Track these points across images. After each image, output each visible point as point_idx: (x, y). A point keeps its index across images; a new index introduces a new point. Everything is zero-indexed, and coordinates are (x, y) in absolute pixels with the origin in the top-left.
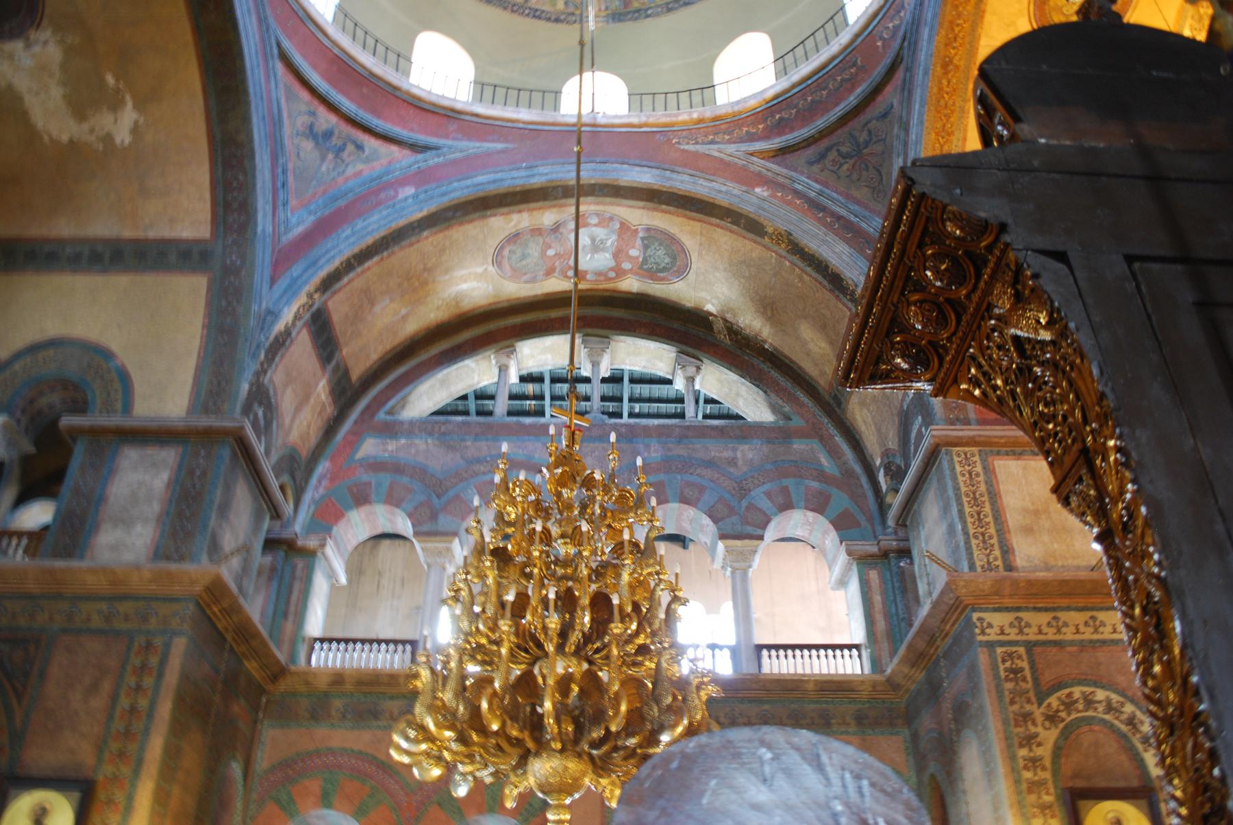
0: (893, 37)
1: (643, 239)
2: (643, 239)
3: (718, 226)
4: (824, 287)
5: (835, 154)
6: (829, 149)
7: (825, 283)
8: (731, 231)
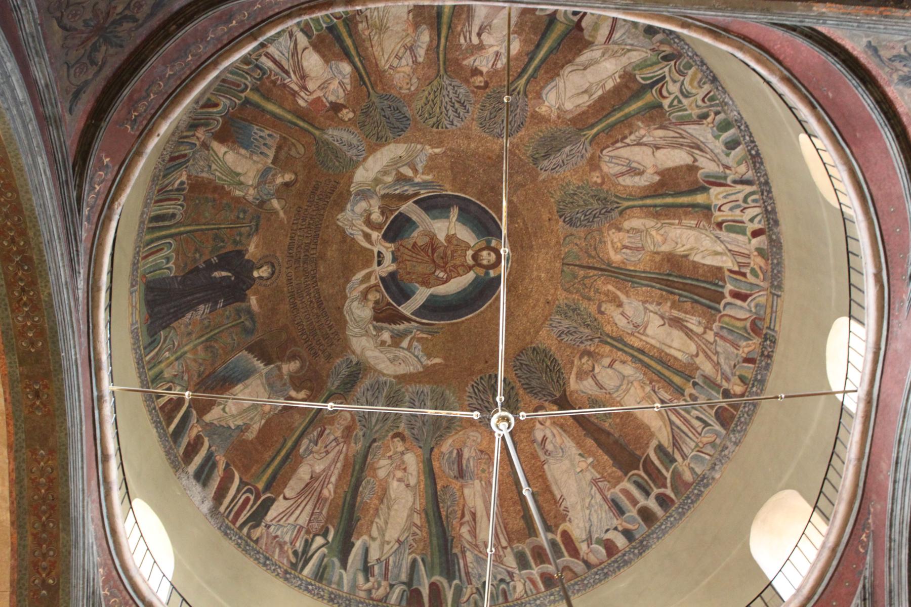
5: (138, 16)
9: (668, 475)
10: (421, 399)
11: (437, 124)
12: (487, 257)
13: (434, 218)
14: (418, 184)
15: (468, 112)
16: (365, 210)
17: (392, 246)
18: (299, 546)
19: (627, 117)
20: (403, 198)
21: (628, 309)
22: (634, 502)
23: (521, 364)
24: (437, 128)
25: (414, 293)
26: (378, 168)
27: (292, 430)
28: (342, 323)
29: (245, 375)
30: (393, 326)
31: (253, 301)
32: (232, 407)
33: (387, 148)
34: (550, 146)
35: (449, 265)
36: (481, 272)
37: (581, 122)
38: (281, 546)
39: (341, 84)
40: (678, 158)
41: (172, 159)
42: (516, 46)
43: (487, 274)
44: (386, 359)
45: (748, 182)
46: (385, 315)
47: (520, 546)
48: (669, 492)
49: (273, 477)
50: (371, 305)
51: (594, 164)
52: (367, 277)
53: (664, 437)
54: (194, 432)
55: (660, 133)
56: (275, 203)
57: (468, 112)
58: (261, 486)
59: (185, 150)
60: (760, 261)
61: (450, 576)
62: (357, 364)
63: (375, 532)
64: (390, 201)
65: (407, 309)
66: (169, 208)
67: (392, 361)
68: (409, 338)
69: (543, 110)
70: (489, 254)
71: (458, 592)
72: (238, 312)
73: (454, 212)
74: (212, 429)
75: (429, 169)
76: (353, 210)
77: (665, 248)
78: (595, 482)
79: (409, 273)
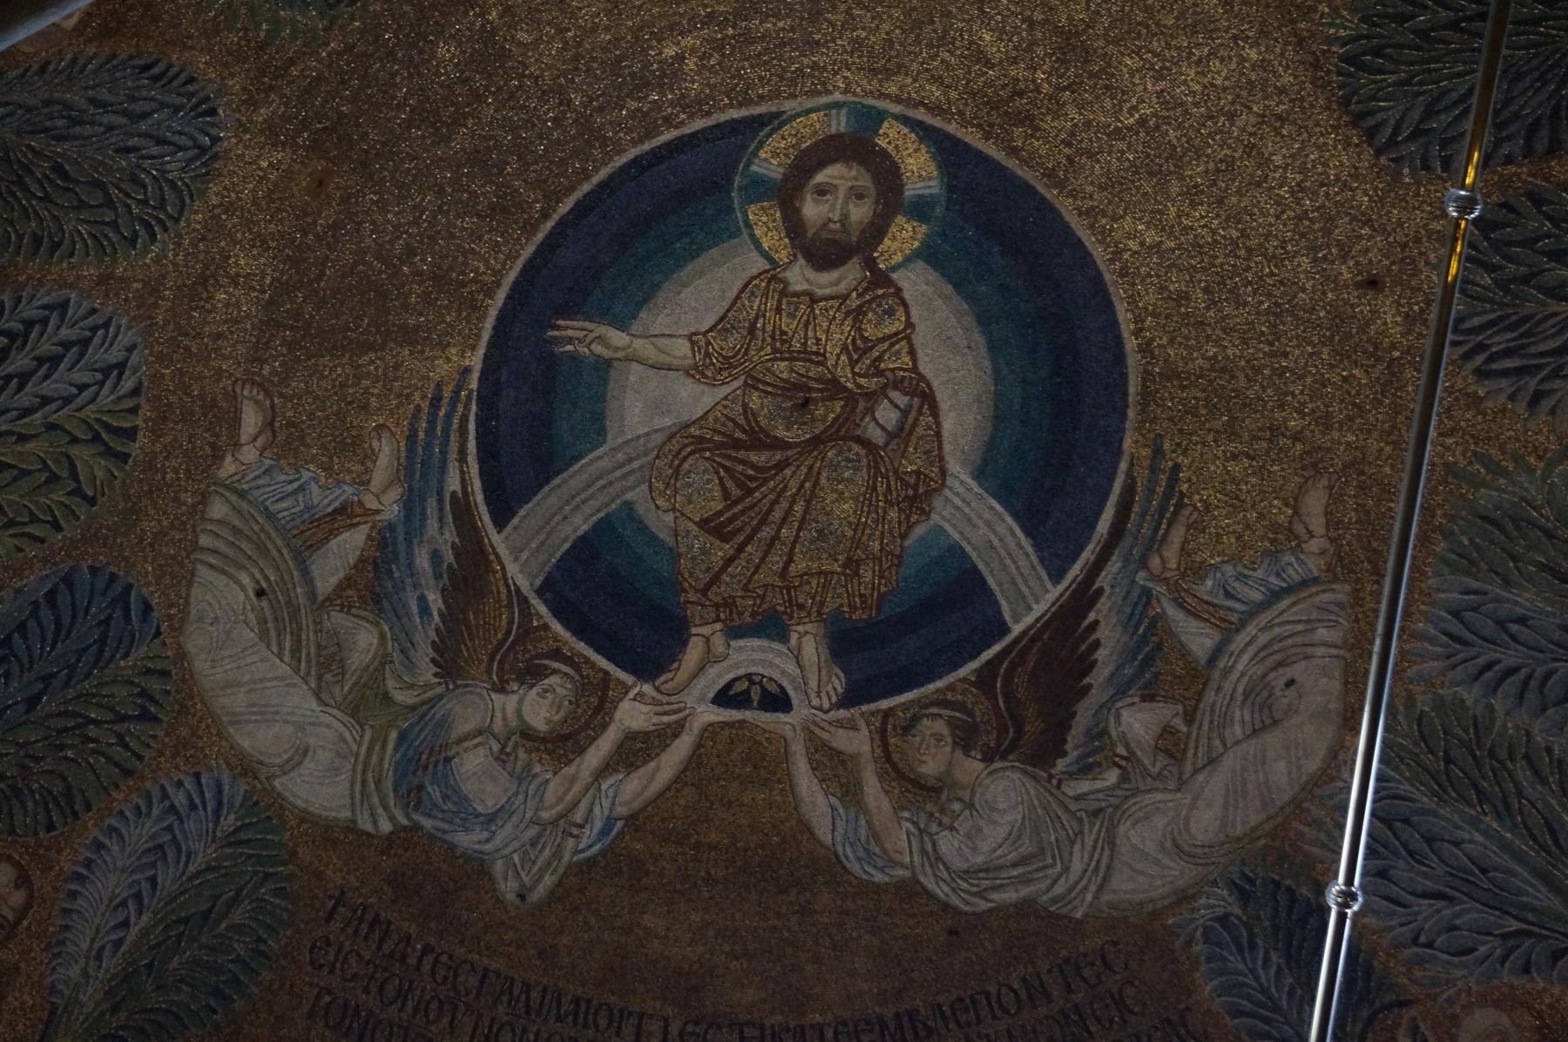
10: (1490, 628)
11: (110, 439)
12: (836, 200)
13: (596, 428)
14: (412, 505)
15: (63, 306)
16: (502, 757)
17: (704, 635)
20: (471, 573)
23: (1417, 134)
24: (131, 434)
25: (956, 551)
26: (300, 701)
28: (1031, 923)
30: (1098, 677)
33: (201, 664)
35: (844, 374)
43: (920, 210)
44: (1252, 747)
46: (1038, 704)
50: (972, 766)
52: (835, 768)
57: (63, 306)
62: (1244, 897)
64: (478, 634)
65: (1027, 598)
67: (1267, 720)
68: (1173, 612)
70: (821, 191)
73: (581, 336)
76: (491, 819)
79: (852, 564)
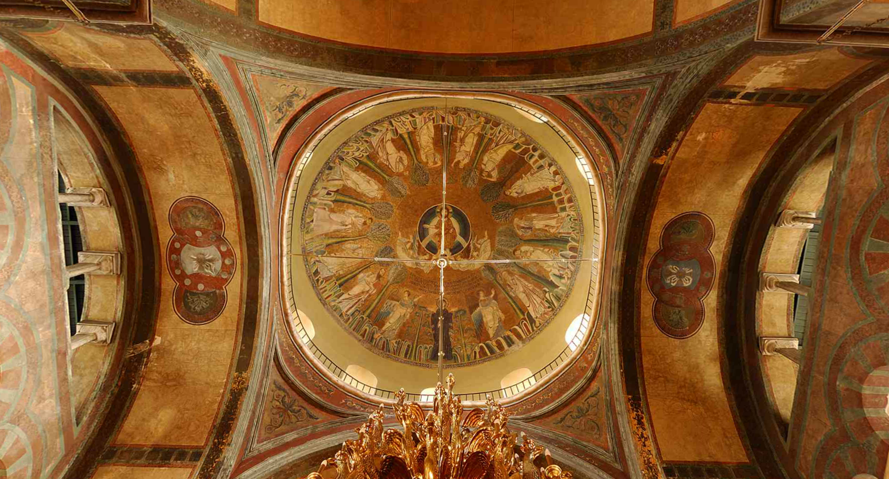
0: (349, 408)
1: (214, 293)
2: (214, 293)
3: (236, 341)
4: (215, 421)
6: (284, 390)
7: (219, 421)
8: (234, 350)
9: (524, 147)
18: (547, 305)
19: (376, 166)
20: (419, 246)
21: (461, 158)
22: (536, 161)
27: (505, 298)
29: (481, 317)
31: (453, 310)
32: (490, 324)
34: (395, 192)
36: (450, 215)
37: (382, 182)
38: (545, 313)
39: (368, 276)
40: (390, 148)
41: (383, 349)
42: (351, 211)
45: (391, 123)
46: (467, 254)
47: (558, 210)
48: (531, 147)
49: (520, 310)
51: (400, 175)
53: (510, 147)
54: (494, 343)
55: (380, 154)
56: (416, 300)
58: (522, 317)
59: (381, 343)
60: (425, 114)
61: (567, 241)
63: (549, 270)
64: (421, 252)
65: (465, 245)
66: (403, 350)
69: (379, 196)
71: (573, 239)
72: (456, 317)
73: (426, 226)
74: (496, 334)
75: (408, 237)
77: (432, 146)
78: (532, 175)
